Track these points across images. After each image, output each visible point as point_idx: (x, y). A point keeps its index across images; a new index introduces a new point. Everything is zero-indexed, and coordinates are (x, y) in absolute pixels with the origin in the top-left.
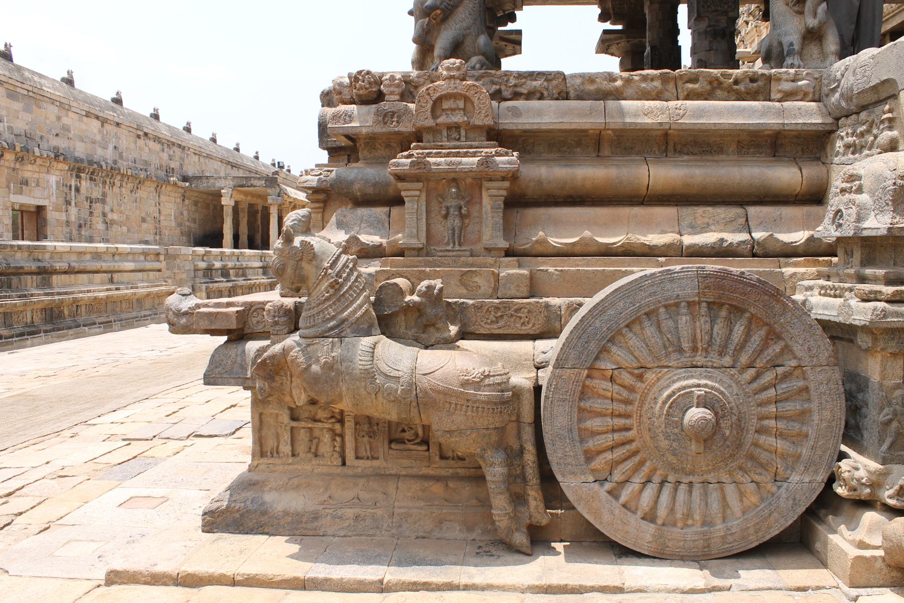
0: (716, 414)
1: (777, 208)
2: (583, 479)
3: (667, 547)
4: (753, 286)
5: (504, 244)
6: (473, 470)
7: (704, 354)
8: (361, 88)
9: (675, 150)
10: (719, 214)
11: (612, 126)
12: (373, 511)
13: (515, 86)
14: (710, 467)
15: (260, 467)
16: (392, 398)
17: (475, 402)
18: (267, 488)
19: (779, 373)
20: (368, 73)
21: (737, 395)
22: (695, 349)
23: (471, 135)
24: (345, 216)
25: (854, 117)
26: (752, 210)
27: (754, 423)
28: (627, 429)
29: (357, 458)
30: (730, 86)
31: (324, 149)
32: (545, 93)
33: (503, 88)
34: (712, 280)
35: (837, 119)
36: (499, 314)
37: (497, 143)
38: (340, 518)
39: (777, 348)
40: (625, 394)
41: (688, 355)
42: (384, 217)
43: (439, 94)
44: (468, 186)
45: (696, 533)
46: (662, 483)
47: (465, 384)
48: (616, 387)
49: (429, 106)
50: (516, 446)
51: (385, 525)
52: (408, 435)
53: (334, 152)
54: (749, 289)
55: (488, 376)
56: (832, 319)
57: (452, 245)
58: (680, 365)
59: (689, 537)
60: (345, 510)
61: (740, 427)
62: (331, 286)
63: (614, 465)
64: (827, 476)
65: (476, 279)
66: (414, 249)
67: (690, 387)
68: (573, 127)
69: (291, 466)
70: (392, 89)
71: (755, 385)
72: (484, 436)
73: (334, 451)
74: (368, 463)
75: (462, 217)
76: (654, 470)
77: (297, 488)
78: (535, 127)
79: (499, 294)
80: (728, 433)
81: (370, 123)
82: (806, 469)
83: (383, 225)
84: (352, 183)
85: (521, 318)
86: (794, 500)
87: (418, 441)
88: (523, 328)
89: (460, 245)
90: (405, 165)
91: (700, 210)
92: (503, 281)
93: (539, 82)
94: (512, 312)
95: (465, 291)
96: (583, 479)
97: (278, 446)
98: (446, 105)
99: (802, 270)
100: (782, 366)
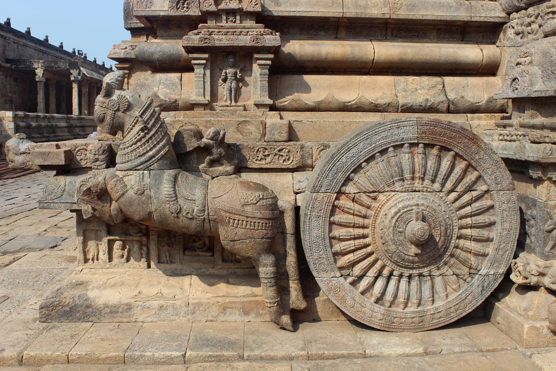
0: (430, 225)
2: (333, 274)
4: (457, 132)
5: (270, 102)
6: (247, 270)
7: (421, 182)
11: (348, 15)
12: (173, 302)
18: (90, 287)
21: (445, 211)
22: (413, 179)
24: (147, 80)
26: (448, 80)
28: (364, 237)
31: (128, 29)
34: (428, 127)
35: (509, 14)
36: (267, 153)
38: (148, 308)
39: (471, 177)
40: (363, 211)
41: (409, 183)
42: (177, 81)
44: (242, 56)
45: (414, 312)
48: (357, 207)
51: (183, 312)
52: (197, 244)
53: (135, 32)
54: (454, 134)
55: (263, 199)
56: (510, 157)
57: (229, 102)
58: (404, 190)
60: (152, 302)
62: (142, 130)
64: (506, 269)
67: (411, 206)
68: (319, 15)
71: (457, 204)
72: (259, 244)
75: (238, 81)
76: (383, 267)
78: (292, 14)
79: (266, 138)
82: (492, 264)
83: (176, 87)
85: (282, 156)
87: (204, 249)
88: (285, 163)
89: (236, 101)
90: (194, 40)
91: (411, 78)
94: (276, 151)
96: (333, 274)
99: (483, 122)
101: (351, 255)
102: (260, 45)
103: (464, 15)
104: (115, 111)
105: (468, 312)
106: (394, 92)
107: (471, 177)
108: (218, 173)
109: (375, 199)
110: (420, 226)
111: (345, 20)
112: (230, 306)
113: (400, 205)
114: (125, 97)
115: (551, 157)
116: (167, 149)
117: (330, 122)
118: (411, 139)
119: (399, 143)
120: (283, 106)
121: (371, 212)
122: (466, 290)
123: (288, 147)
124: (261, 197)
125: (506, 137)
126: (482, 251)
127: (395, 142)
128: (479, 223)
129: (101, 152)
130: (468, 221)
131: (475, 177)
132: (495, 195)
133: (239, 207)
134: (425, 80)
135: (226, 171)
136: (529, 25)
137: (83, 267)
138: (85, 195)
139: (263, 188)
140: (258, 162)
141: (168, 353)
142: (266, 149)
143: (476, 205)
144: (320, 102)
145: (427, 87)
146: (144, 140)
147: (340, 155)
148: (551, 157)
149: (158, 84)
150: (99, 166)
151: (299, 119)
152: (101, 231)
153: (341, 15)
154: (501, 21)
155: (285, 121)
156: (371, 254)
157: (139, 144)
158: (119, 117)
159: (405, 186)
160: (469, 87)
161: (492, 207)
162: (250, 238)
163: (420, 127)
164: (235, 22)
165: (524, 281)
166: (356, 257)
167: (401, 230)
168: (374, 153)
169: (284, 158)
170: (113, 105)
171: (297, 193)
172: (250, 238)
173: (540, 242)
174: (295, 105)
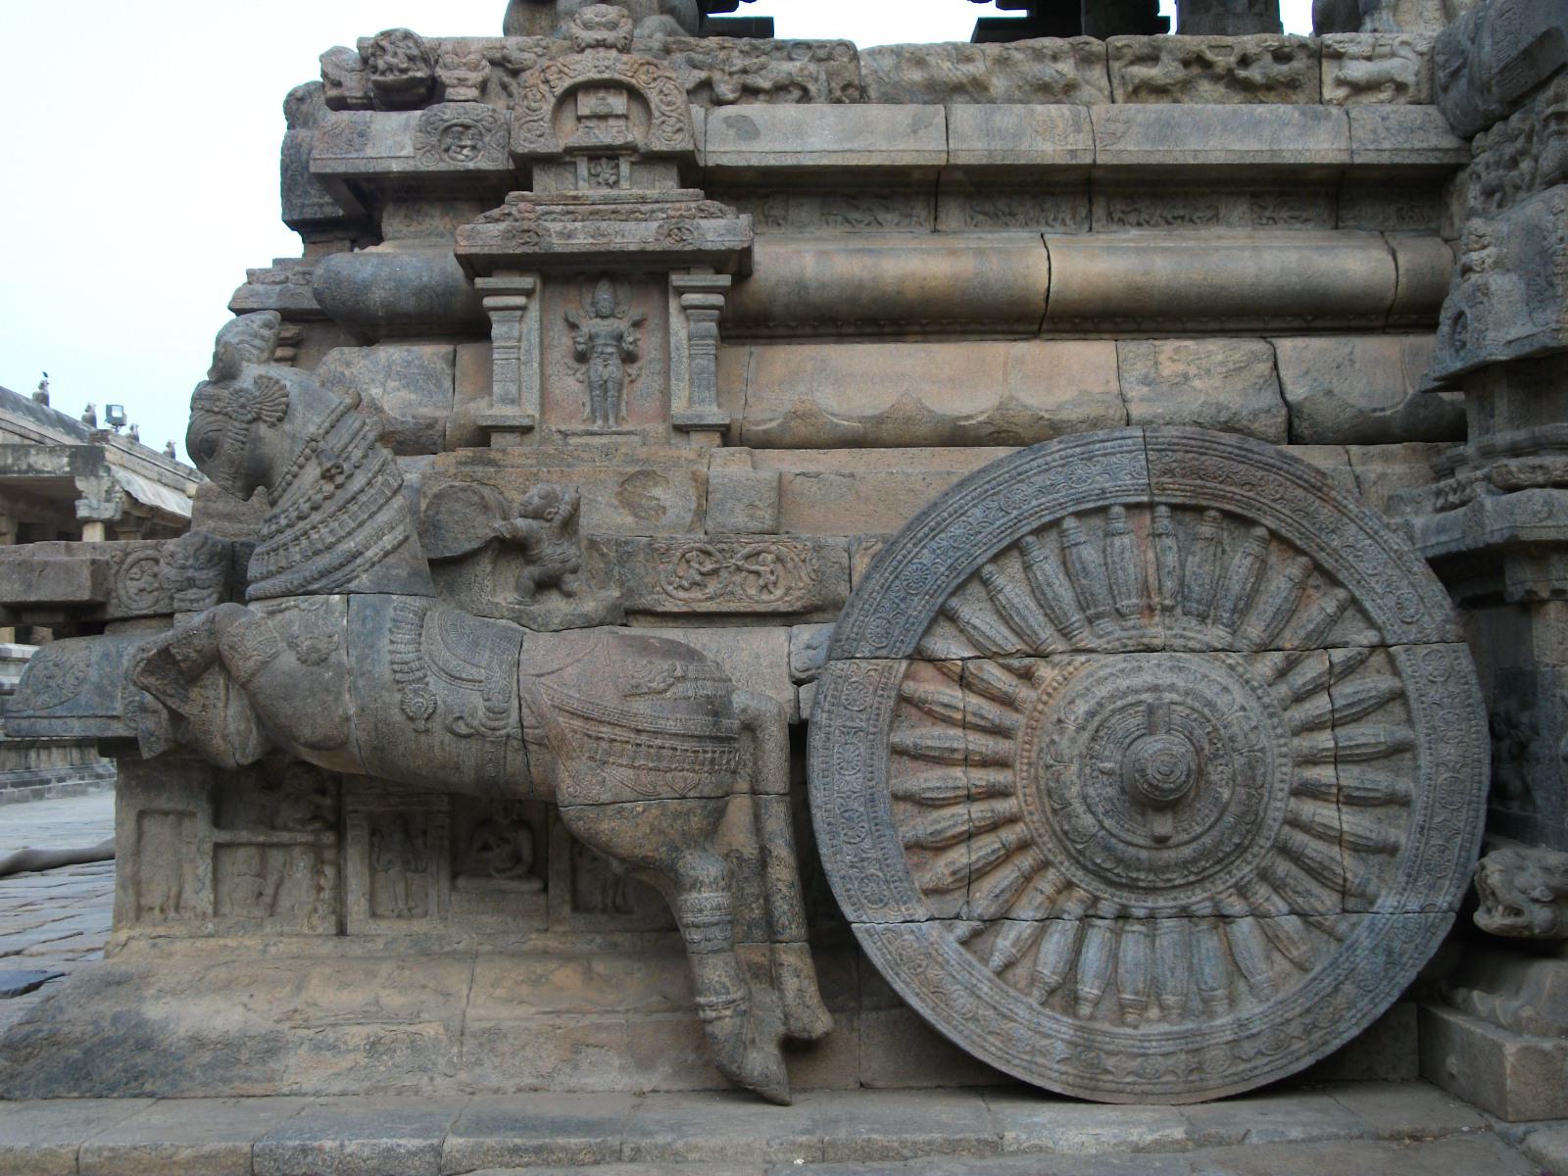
0: (1199, 751)
1: (1343, 340)
3: (1107, 1072)
8: (391, 69)
9: (1110, 216)
10: (1209, 354)
11: (963, 159)
13: (744, 71)
14: (1192, 878)
15: (134, 945)
16: (462, 728)
17: (656, 733)
19: (1335, 660)
20: (407, 35)
23: (643, 174)
25: (1498, 127)
26: (1286, 346)
27: (1282, 775)
29: (374, 915)
30: (1230, 71)
32: (812, 88)
33: (717, 76)
34: (1179, 455)
35: (1468, 138)
36: (709, 566)
37: (702, 193)
40: (992, 712)
42: (441, 366)
43: (567, 83)
45: (1168, 1037)
46: (1086, 919)
47: (634, 693)
48: (974, 701)
49: (547, 107)
50: (750, 851)
51: (442, 1061)
54: (1260, 473)
55: (684, 678)
56: (1453, 547)
59: (1153, 1047)
61: (1252, 780)
62: (327, 476)
63: (970, 878)
64: (1460, 894)
65: (657, 492)
66: (511, 429)
69: (212, 942)
70: (461, 73)
72: (677, 815)
73: (318, 899)
74: (402, 927)
77: (227, 987)
78: (790, 161)
79: (710, 525)
80: (1226, 794)
81: (408, 151)
82: (1412, 879)
83: (439, 384)
84: (366, 286)
85: (758, 574)
86: (1389, 953)
88: (765, 597)
91: (1168, 347)
92: (719, 496)
93: (798, 64)
95: (630, 520)
97: (179, 894)
98: (587, 104)
100: (1345, 645)
101: (962, 849)
102: (689, 248)
103: (1325, 146)
104: (250, 422)
105: (1347, 1037)
106: (1114, 387)
107: (1324, 604)
108: (557, 621)
109: (1026, 676)
110: (1160, 746)
111: (959, 176)
112: (592, 1040)
113: (1102, 692)
114: (277, 382)
115: (1550, 523)
116: (398, 534)
117: (908, 475)
118: (1126, 492)
119: (1091, 505)
120: (765, 432)
121: (1015, 716)
122: (1334, 964)
123: (773, 547)
124: (679, 673)
125: (1452, 498)
126: (1374, 836)
127: (1078, 501)
128: (1358, 746)
129: (203, 558)
130: (1324, 740)
131: (1334, 603)
132: (1402, 657)
133: (610, 700)
134: (1216, 350)
135: (579, 616)
136: (1514, 162)
137: (132, 933)
138: (152, 674)
139: (692, 655)
140: (682, 594)
141: (385, 1142)
142: (708, 553)
143: (1346, 690)
144: (879, 420)
145: (1219, 369)
146: (330, 507)
147: (915, 545)
148: (1550, 523)
149: (380, 377)
150: (197, 601)
151: (812, 468)
152: (192, 815)
153: (941, 160)
154: (1446, 161)
155: (767, 474)
156: (1024, 846)
157: (316, 517)
158: (260, 439)
159: (1116, 635)
160: (1357, 366)
161: (1399, 696)
162: (646, 797)
163: (1153, 456)
164: (616, 184)
165: (1509, 921)
166: (974, 858)
167: (1109, 765)
168: (1017, 536)
169: (761, 582)
170: (243, 406)
171: (799, 683)
172: (646, 797)
173: (1554, 798)
174: (802, 430)
